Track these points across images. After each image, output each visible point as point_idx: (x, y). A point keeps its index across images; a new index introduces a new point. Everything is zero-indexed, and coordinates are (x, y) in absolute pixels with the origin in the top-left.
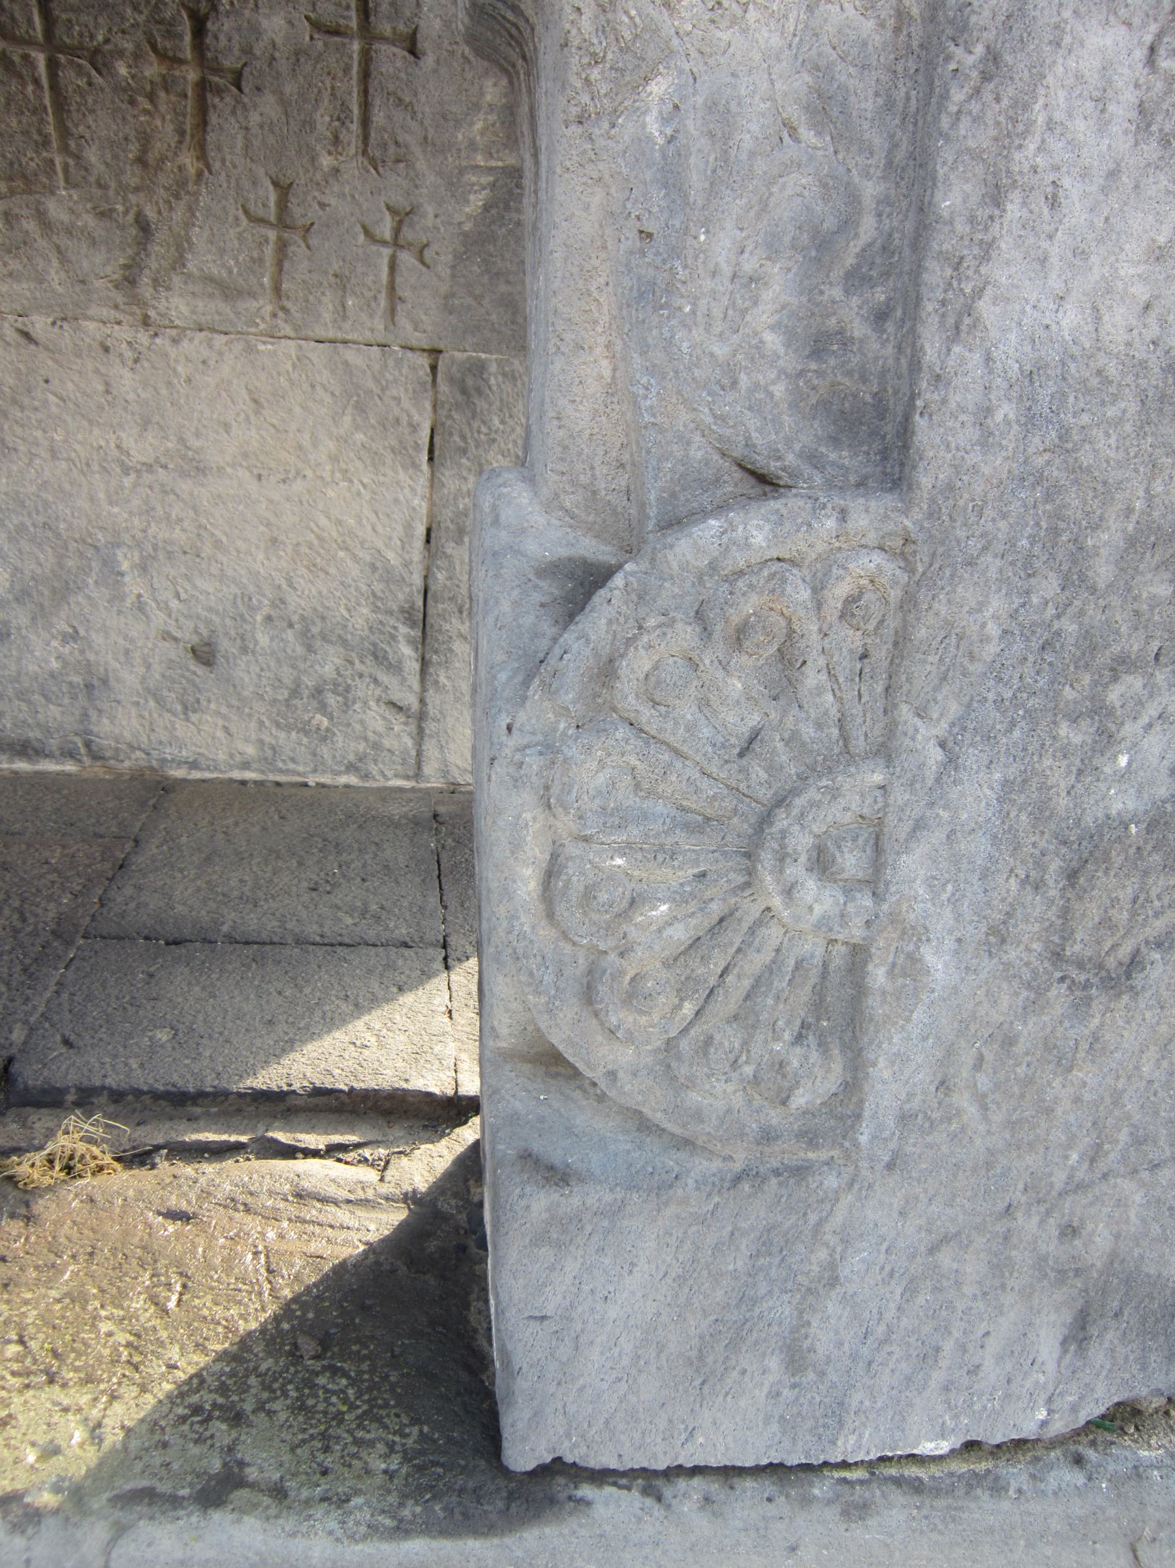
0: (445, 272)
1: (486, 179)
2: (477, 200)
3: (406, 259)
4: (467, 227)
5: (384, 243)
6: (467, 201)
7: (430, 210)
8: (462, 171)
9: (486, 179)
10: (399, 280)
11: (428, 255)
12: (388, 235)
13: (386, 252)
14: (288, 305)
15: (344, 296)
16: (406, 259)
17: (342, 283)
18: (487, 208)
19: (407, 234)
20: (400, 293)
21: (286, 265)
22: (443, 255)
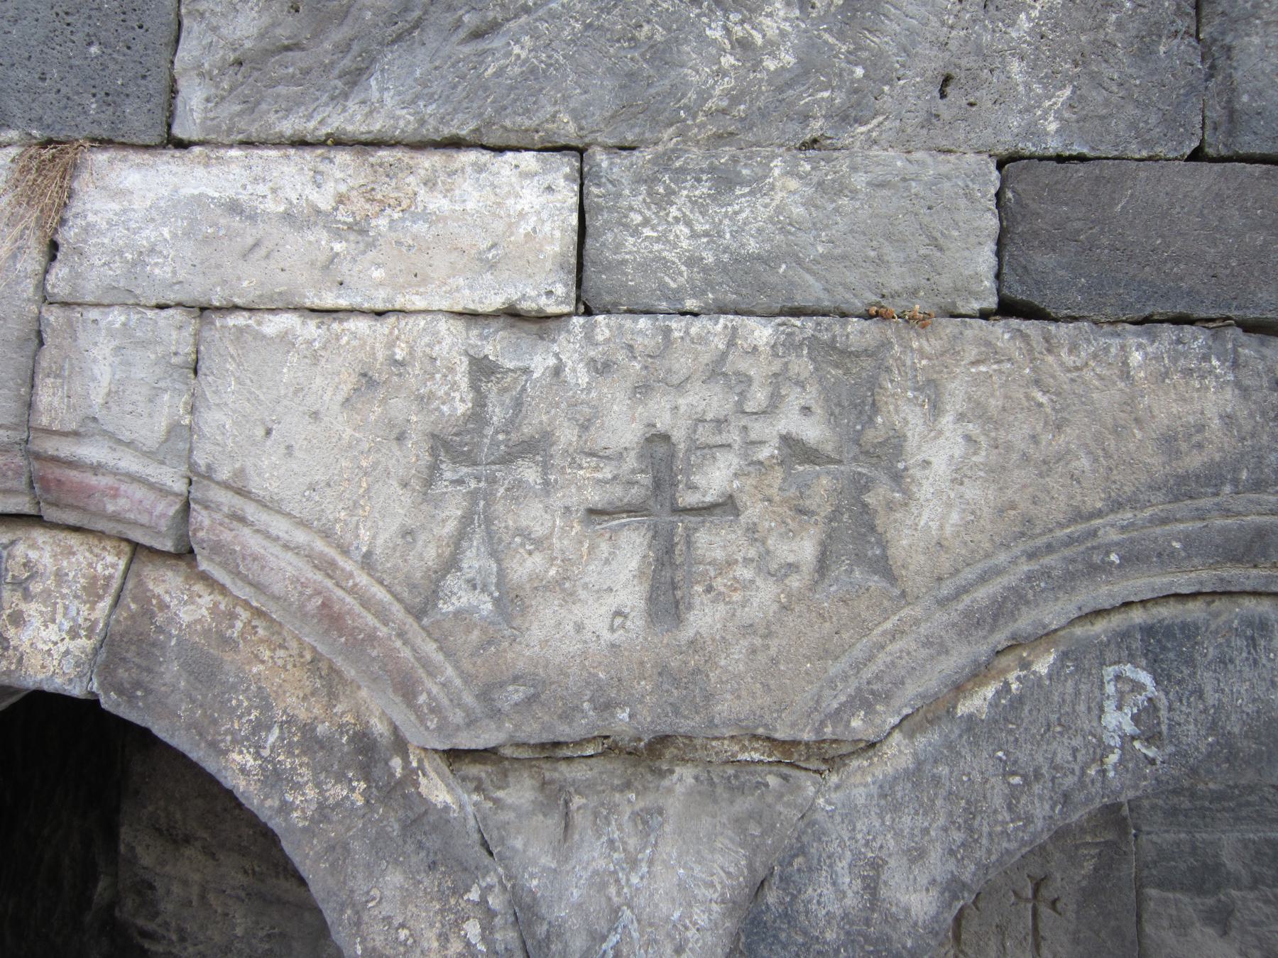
0: (1071, 915)
1: (1094, 851)
2: (1089, 866)
3: (1045, 911)
4: (1084, 883)
5: (1027, 900)
6: (1082, 867)
7: (1058, 876)
8: (1077, 847)
9: (1094, 851)
10: (1041, 925)
11: (1059, 905)
12: (1030, 895)
13: (1030, 906)
14: (966, 949)
15: (1003, 939)
16: (1045, 911)
17: (1001, 930)
18: (1096, 870)
19: (1047, 893)
20: (1042, 933)
21: (964, 922)
22: (1069, 905)
